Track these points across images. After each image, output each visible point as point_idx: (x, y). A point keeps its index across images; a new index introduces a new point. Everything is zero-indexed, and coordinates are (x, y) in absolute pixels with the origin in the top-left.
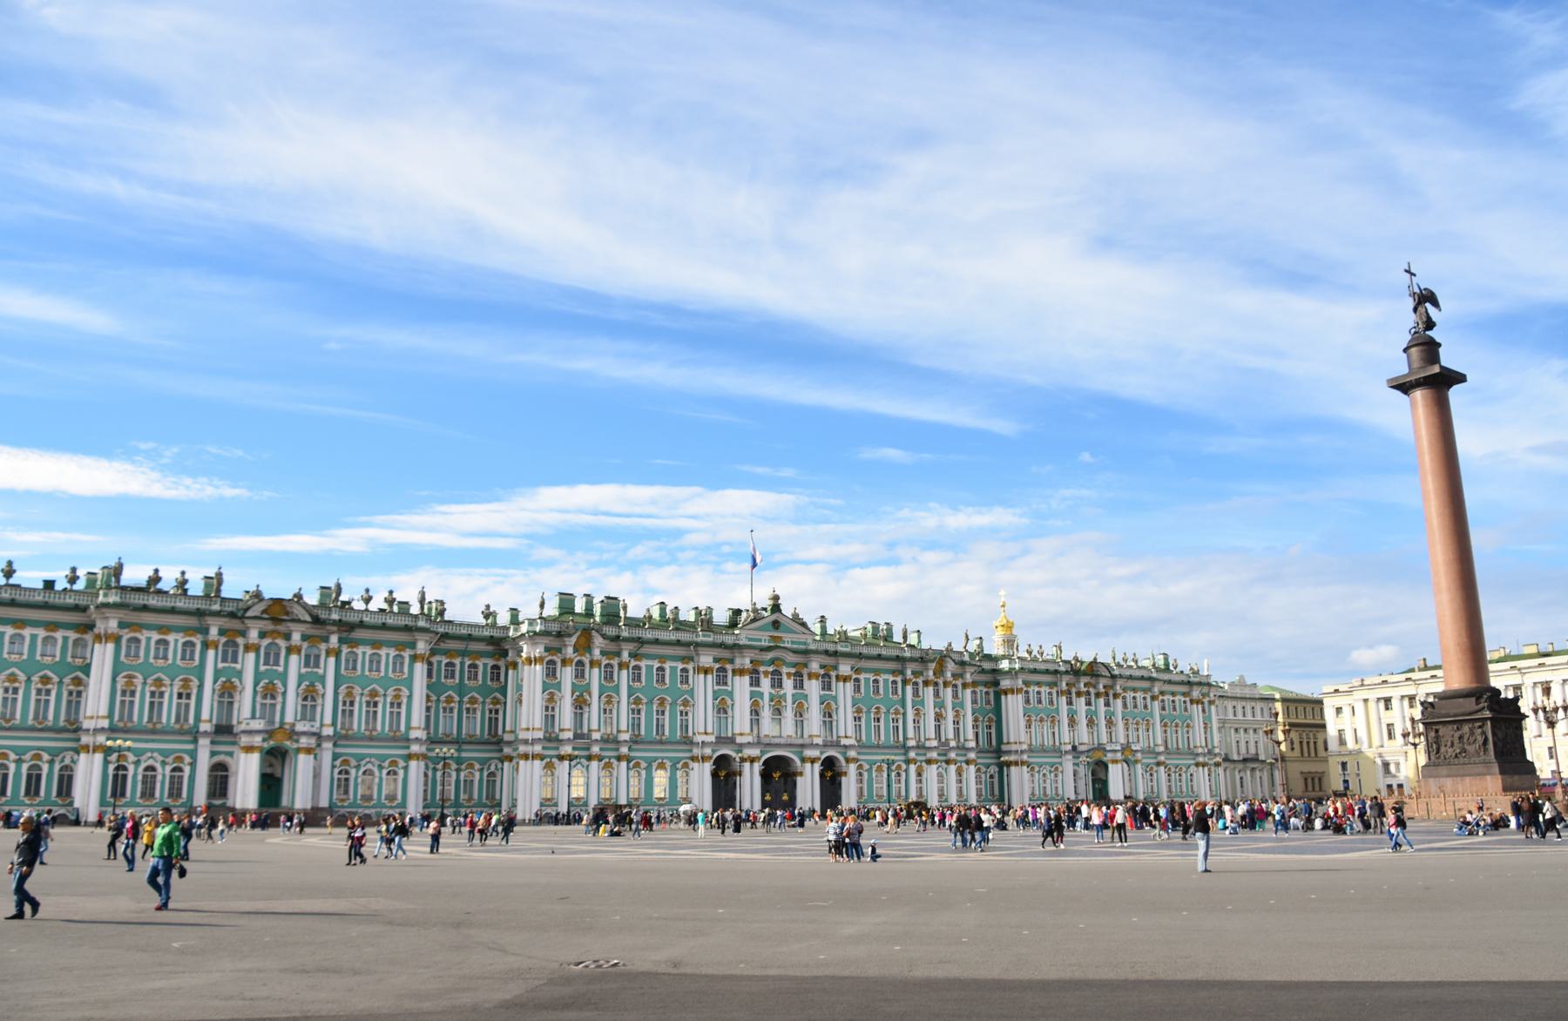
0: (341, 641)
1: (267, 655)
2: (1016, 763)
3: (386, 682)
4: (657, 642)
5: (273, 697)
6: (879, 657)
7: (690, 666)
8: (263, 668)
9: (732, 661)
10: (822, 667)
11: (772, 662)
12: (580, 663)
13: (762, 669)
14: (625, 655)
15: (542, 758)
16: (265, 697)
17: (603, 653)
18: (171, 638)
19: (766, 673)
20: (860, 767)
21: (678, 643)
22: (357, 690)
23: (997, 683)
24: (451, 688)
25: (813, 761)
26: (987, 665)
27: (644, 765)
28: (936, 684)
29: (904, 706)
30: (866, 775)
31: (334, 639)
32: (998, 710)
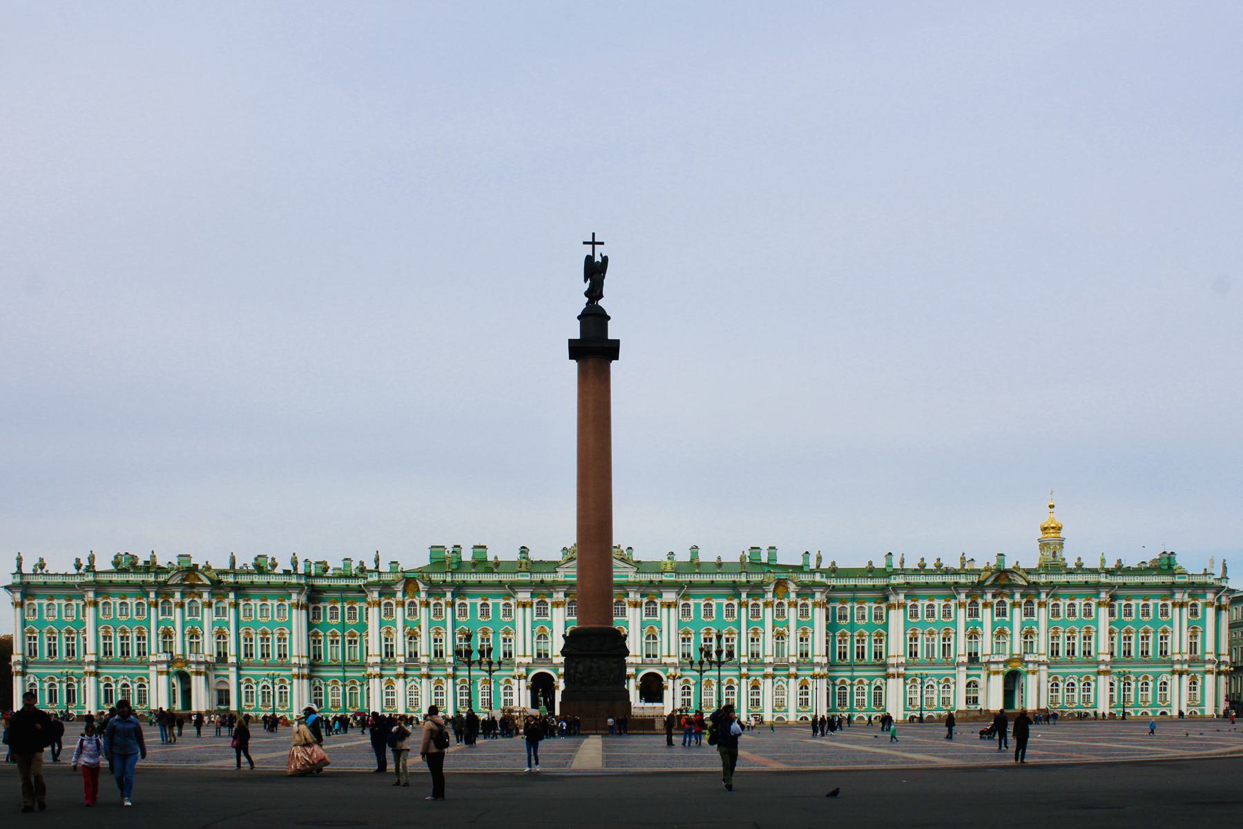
1: (190, 608)
2: (893, 676)
3: (272, 624)
4: (480, 584)
5: (197, 637)
6: (712, 584)
7: (512, 602)
9: (551, 596)
10: (642, 596)
12: (412, 604)
16: (192, 637)
17: (429, 594)
20: (686, 681)
21: (500, 584)
22: (252, 631)
23: (886, 599)
24: (335, 626)
26: (880, 582)
28: (781, 604)
29: (739, 628)
32: (886, 626)
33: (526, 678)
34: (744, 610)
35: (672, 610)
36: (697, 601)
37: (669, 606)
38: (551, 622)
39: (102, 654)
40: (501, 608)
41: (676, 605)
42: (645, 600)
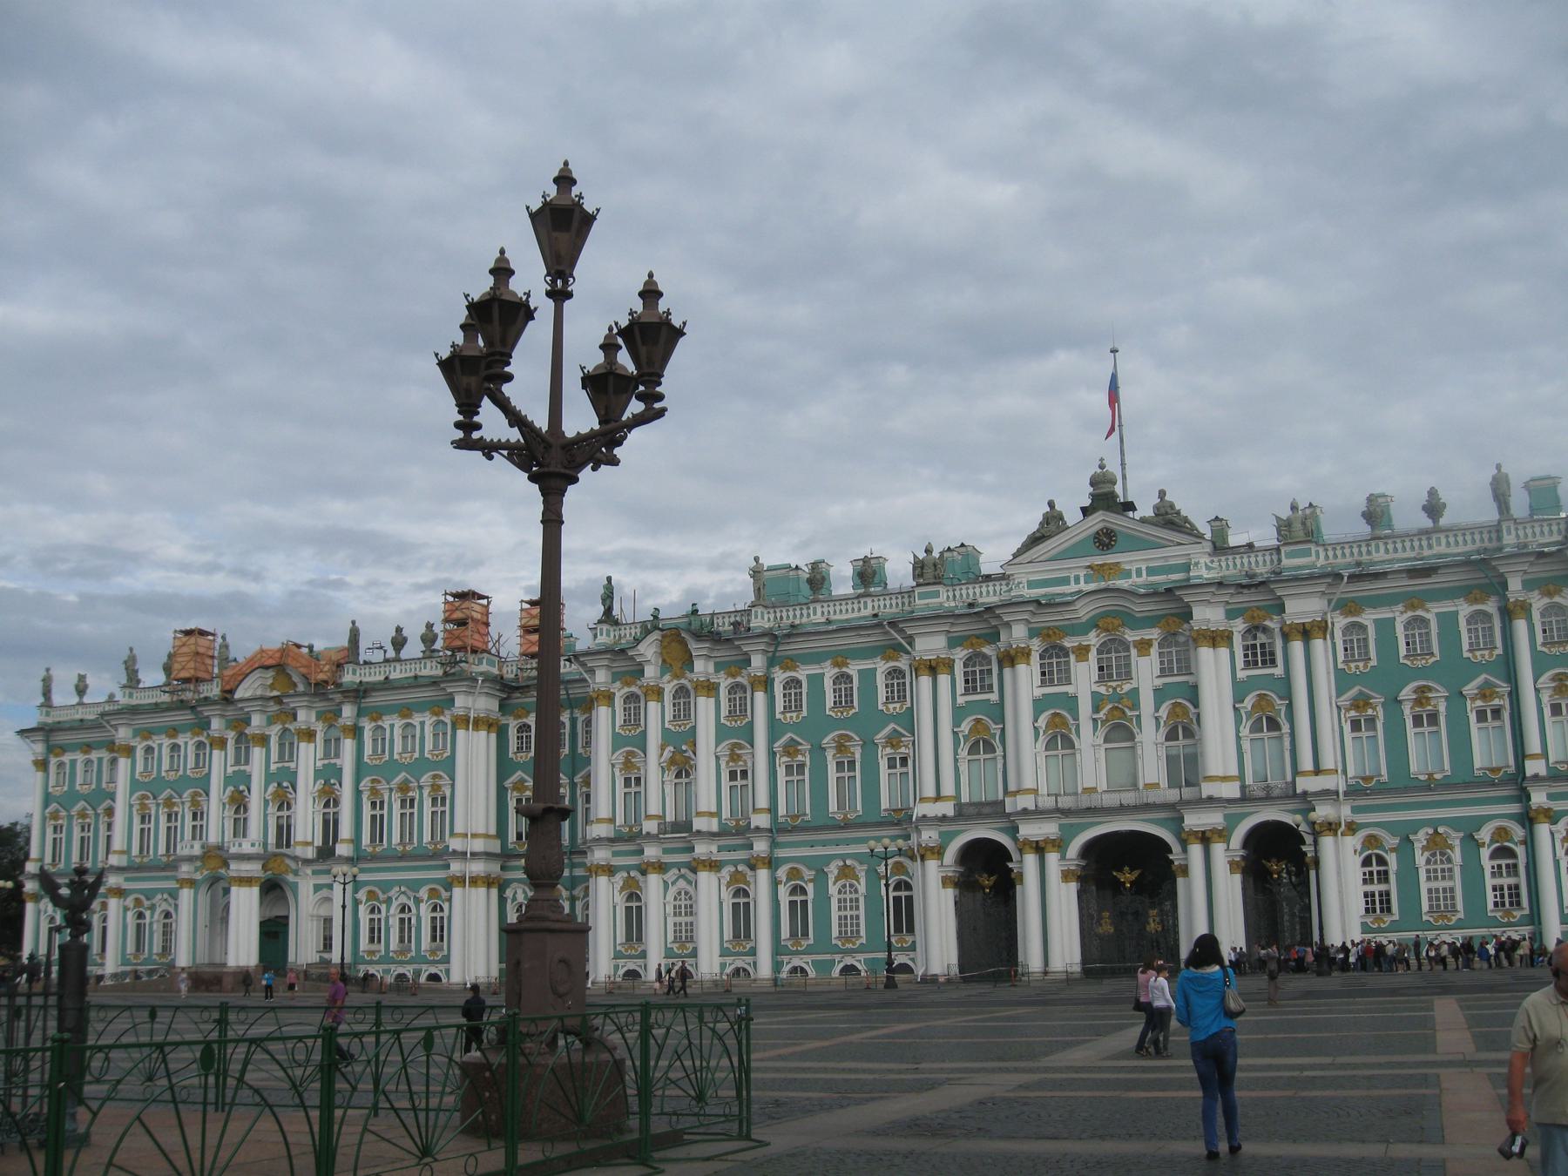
0: (360, 714)
1: (282, 746)
3: (421, 765)
7: (903, 663)
8: (273, 767)
9: (993, 637)
10: (1231, 615)
11: (1093, 624)
13: (1068, 643)
14: (758, 662)
15: (610, 870)
18: (180, 741)
19: (1082, 652)
22: (383, 786)
25: (1205, 839)
27: (808, 874)
30: (1392, 859)
31: (348, 711)
33: (939, 852)
34: (1521, 626)
35: (1318, 645)
36: (1384, 614)
37: (1306, 633)
38: (1001, 704)
39: (135, 851)
40: (881, 681)
41: (1323, 628)
42: (1239, 626)
